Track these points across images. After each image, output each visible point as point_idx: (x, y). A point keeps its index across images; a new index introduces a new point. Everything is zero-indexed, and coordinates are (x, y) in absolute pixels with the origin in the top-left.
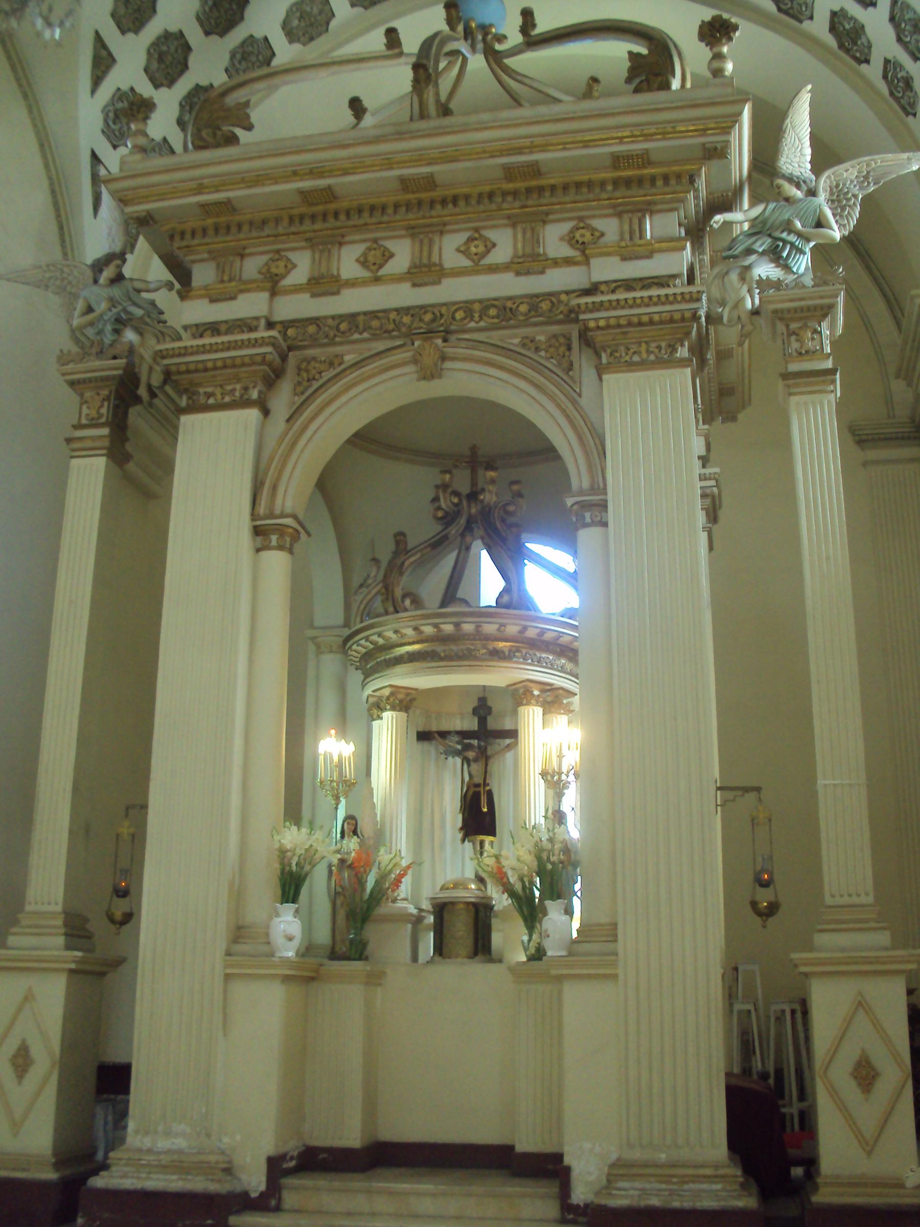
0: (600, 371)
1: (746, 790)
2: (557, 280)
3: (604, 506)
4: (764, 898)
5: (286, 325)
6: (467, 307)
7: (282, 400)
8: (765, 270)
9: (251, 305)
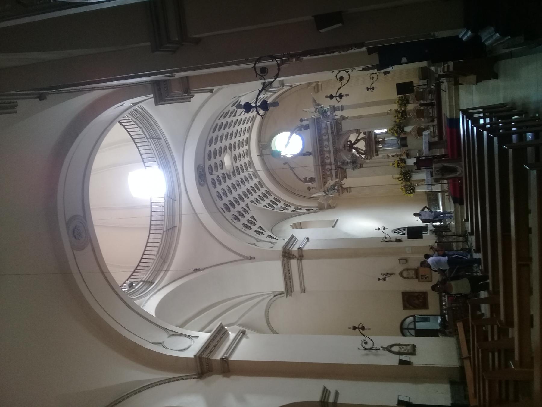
2: (330, 137)
9: (333, 172)
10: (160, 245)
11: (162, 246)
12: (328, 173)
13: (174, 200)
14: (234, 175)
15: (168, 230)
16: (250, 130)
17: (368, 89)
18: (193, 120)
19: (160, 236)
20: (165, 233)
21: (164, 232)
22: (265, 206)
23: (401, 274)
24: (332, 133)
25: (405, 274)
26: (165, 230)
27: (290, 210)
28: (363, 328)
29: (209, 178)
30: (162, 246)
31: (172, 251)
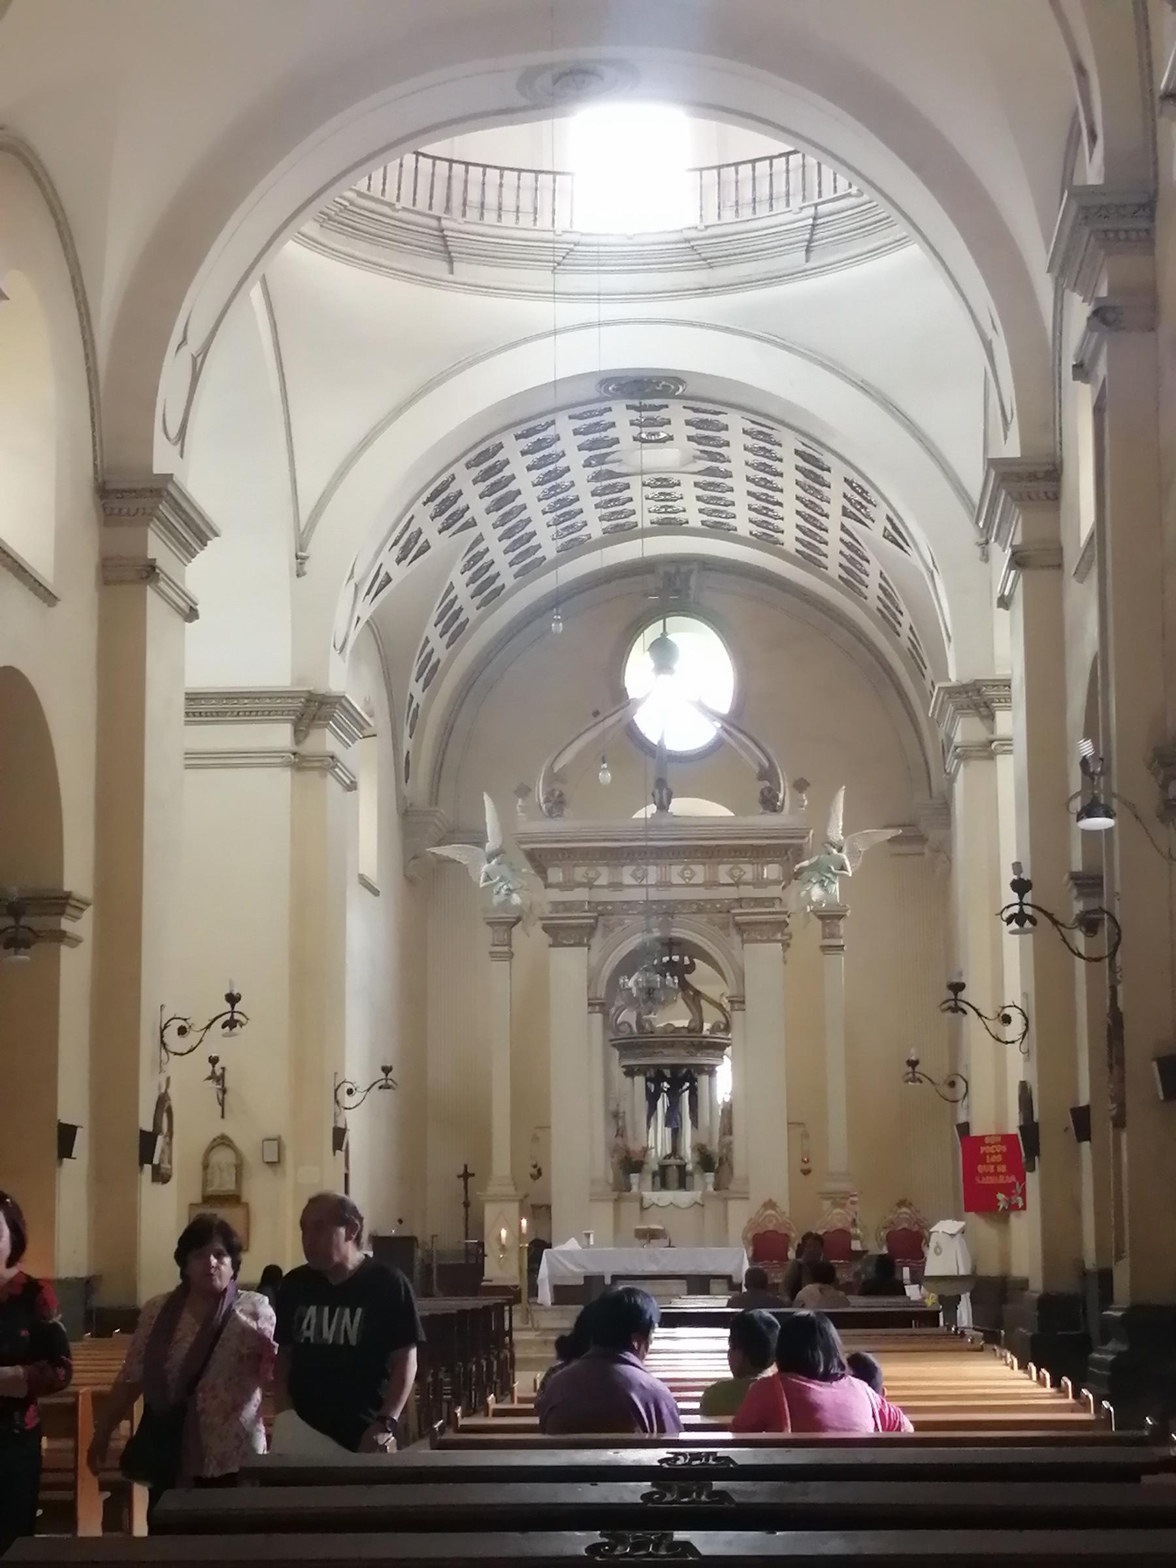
0: (743, 942)
1: (799, 1124)
3: (743, 1002)
4: (806, 1167)
5: (599, 903)
6: (683, 902)
7: (597, 941)
8: (816, 893)
9: (580, 894)
10: (391, 205)
11: (386, 210)
12: (580, 873)
13: (556, 267)
14: (596, 477)
16: (767, 540)
17: (913, 1064)
18: (864, 388)
19: (422, 205)
20: (434, 223)
21: (439, 219)
22: (452, 587)
23: (223, 1141)
24: (739, 901)
25: (223, 1157)
26: (445, 223)
27: (416, 688)
28: (231, 1024)
30: (386, 210)
31: (361, 249)
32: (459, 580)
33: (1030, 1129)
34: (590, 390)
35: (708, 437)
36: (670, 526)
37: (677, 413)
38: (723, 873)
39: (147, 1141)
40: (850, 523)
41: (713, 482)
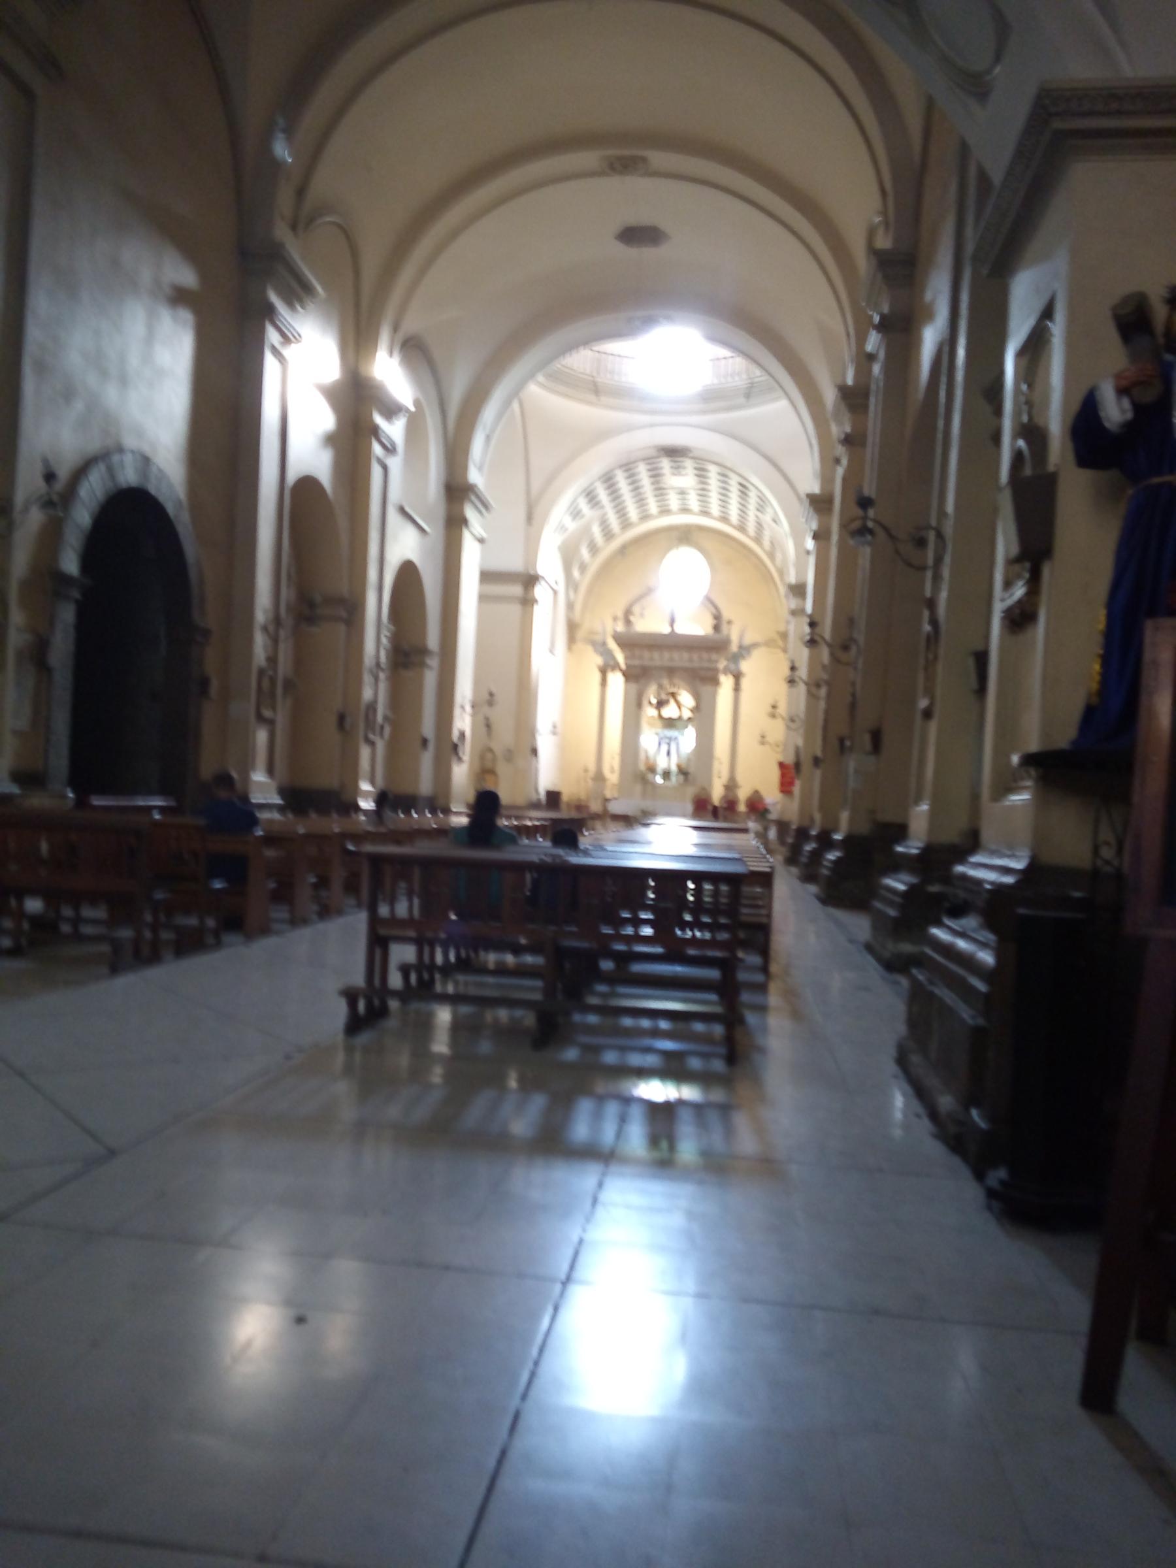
9: (636, 662)
12: (637, 652)
15: (595, 384)
16: (724, 519)
25: (489, 756)
27: (576, 573)
29: (665, 464)
32: (596, 530)
33: (797, 765)
34: (653, 453)
35: (701, 474)
36: (685, 510)
37: (689, 464)
38: (695, 656)
39: (455, 747)
40: (759, 514)
41: (703, 494)
